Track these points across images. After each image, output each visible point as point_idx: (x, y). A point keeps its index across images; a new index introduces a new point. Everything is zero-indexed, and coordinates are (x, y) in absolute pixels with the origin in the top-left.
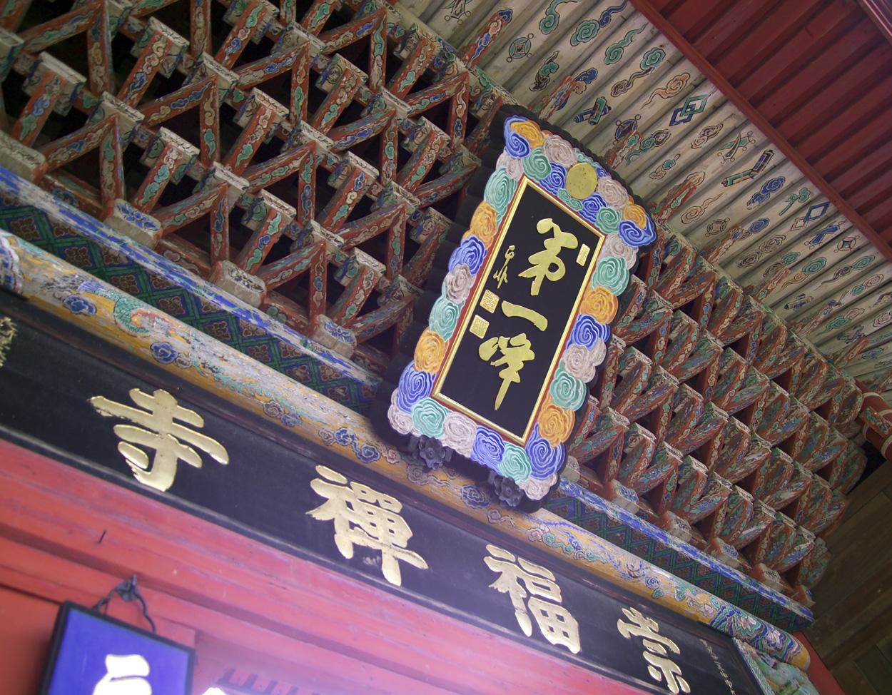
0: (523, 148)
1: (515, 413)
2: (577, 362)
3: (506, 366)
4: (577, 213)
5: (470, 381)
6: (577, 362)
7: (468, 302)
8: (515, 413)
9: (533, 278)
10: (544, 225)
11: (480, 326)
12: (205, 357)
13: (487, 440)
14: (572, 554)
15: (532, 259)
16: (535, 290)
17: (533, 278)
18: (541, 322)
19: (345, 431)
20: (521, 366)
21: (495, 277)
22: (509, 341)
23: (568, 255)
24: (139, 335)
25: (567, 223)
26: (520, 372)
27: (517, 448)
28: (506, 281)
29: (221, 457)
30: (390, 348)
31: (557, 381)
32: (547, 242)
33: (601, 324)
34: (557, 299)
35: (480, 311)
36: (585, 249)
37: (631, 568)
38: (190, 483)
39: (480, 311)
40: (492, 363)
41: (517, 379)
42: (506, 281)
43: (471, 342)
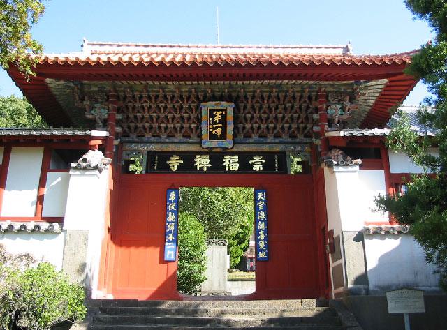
0: (204, 106)
1: (223, 137)
2: (230, 128)
5: (213, 137)
8: (223, 137)
10: (215, 113)
18: (221, 125)
30: (200, 136)
34: (223, 121)
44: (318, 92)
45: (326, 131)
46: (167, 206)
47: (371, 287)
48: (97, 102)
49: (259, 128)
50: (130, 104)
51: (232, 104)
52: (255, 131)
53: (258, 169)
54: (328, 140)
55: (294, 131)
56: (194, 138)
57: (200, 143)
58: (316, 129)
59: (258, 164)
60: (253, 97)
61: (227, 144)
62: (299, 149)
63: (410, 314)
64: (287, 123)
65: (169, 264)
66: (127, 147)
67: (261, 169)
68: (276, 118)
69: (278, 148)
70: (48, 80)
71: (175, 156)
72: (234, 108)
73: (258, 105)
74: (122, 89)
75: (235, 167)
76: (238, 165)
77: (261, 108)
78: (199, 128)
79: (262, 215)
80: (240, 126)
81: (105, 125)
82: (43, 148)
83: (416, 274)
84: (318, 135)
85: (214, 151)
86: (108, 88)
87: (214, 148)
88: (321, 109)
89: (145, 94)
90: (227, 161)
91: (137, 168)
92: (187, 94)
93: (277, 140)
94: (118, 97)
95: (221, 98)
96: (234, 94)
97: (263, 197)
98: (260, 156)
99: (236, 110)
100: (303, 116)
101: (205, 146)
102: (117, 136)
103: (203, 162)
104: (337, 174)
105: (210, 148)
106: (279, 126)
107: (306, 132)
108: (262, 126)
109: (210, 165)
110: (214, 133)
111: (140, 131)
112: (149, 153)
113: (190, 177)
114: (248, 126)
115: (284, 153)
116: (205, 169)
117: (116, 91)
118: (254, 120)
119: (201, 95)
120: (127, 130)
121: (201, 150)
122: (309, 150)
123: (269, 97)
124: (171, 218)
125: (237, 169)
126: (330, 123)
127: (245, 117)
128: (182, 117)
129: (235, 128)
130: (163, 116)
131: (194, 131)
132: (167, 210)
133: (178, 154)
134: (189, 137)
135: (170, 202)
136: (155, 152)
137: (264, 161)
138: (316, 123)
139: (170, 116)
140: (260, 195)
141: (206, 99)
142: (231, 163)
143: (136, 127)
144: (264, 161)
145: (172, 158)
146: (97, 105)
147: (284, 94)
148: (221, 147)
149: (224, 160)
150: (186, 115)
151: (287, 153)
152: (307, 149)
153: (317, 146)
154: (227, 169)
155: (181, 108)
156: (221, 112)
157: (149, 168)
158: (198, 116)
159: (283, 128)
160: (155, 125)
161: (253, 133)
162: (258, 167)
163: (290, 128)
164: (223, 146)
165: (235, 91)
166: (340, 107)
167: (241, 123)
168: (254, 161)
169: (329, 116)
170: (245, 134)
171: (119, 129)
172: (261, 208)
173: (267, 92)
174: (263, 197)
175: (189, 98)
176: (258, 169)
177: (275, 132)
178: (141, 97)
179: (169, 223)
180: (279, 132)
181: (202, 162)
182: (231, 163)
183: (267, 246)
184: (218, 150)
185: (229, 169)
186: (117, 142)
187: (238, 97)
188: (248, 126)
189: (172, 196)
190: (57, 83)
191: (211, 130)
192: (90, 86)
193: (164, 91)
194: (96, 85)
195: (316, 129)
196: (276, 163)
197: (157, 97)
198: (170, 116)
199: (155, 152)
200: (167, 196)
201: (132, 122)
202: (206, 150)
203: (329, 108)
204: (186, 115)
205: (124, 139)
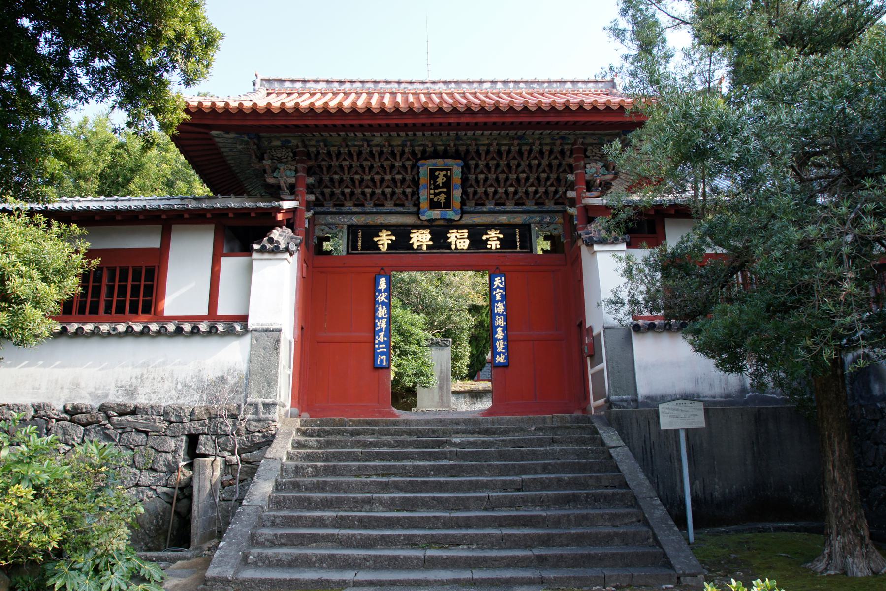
0: (423, 165)
1: (448, 205)
2: (457, 193)
5: (434, 205)
6: (457, 193)
10: (436, 174)
18: (445, 190)
25: (442, 170)
29: (394, 238)
30: (417, 204)
34: (448, 184)
43: (431, 200)
44: (573, 144)
45: (584, 198)
46: (375, 297)
47: (640, 398)
48: (280, 160)
49: (495, 192)
50: (324, 163)
51: (460, 162)
52: (491, 197)
53: (494, 247)
54: (587, 208)
55: (540, 197)
57: (417, 214)
58: (571, 194)
59: (493, 240)
60: (488, 152)
62: (548, 219)
63: (687, 431)
64: (532, 185)
65: (381, 371)
66: (322, 219)
67: (498, 246)
68: (518, 180)
69: (519, 219)
70: (214, 133)
71: (384, 231)
72: (462, 168)
73: (495, 162)
74: (313, 143)
75: (464, 244)
76: (467, 242)
77: (498, 166)
78: (416, 193)
79: (500, 308)
80: (470, 190)
81: (293, 190)
82: (213, 226)
83: (697, 382)
84: (573, 202)
85: (437, 223)
86: (294, 142)
87: (436, 219)
88: (577, 168)
89: (344, 150)
91: (336, 245)
92: (400, 148)
93: (520, 209)
94: (308, 154)
95: (445, 155)
96: (463, 149)
97: (501, 283)
98: (496, 229)
99: (466, 169)
100: (553, 176)
101: (423, 218)
102: (309, 206)
103: (421, 238)
104: (598, 255)
106: (521, 190)
107: (557, 196)
108: (500, 190)
109: (431, 243)
110: (435, 200)
111: (338, 198)
112: (349, 227)
113: (404, 257)
114: (481, 190)
115: (529, 225)
116: (424, 248)
117: (305, 146)
118: (489, 182)
120: (320, 197)
121: (419, 222)
122: (562, 220)
123: (509, 152)
124: (382, 312)
125: (466, 247)
126: (589, 186)
127: (476, 179)
128: (393, 180)
129: (465, 192)
130: (369, 178)
132: (375, 302)
133: (387, 227)
134: (403, 205)
135: (380, 291)
136: (357, 226)
137: (501, 236)
138: (572, 186)
139: (377, 178)
140: (497, 281)
141: (425, 156)
142: (459, 240)
143: (332, 194)
144: (501, 236)
145: (380, 234)
146: (282, 167)
149: (449, 235)
150: (399, 177)
151: (532, 226)
152: (559, 219)
153: (572, 216)
154: (453, 247)
156: (445, 173)
157: (352, 245)
158: (414, 178)
159: (526, 193)
162: (494, 244)
163: (536, 192)
165: (463, 145)
166: (602, 164)
167: (471, 186)
169: (587, 177)
171: (312, 198)
172: (498, 298)
174: (501, 283)
175: (403, 153)
176: (494, 247)
177: (517, 197)
178: (339, 154)
179: (379, 319)
180: (521, 197)
181: (420, 239)
182: (459, 240)
183: (506, 348)
184: (441, 222)
185: (456, 248)
186: (309, 214)
187: (467, 152)
188: (481, 190)
189: (383, 284)
190: (227, 136)
191: (432, 196)
192: (270, 140)
193: (368, 145)
194: (278, 139)
195: (571, 194)
196: (516, 238)
197: (360, 153)
198: (377, 178)
200: (376, 283)
201: (326, 187)
202: (426, 223)
203: (588, 166)
204: (399, 177)
205: (320, 209)
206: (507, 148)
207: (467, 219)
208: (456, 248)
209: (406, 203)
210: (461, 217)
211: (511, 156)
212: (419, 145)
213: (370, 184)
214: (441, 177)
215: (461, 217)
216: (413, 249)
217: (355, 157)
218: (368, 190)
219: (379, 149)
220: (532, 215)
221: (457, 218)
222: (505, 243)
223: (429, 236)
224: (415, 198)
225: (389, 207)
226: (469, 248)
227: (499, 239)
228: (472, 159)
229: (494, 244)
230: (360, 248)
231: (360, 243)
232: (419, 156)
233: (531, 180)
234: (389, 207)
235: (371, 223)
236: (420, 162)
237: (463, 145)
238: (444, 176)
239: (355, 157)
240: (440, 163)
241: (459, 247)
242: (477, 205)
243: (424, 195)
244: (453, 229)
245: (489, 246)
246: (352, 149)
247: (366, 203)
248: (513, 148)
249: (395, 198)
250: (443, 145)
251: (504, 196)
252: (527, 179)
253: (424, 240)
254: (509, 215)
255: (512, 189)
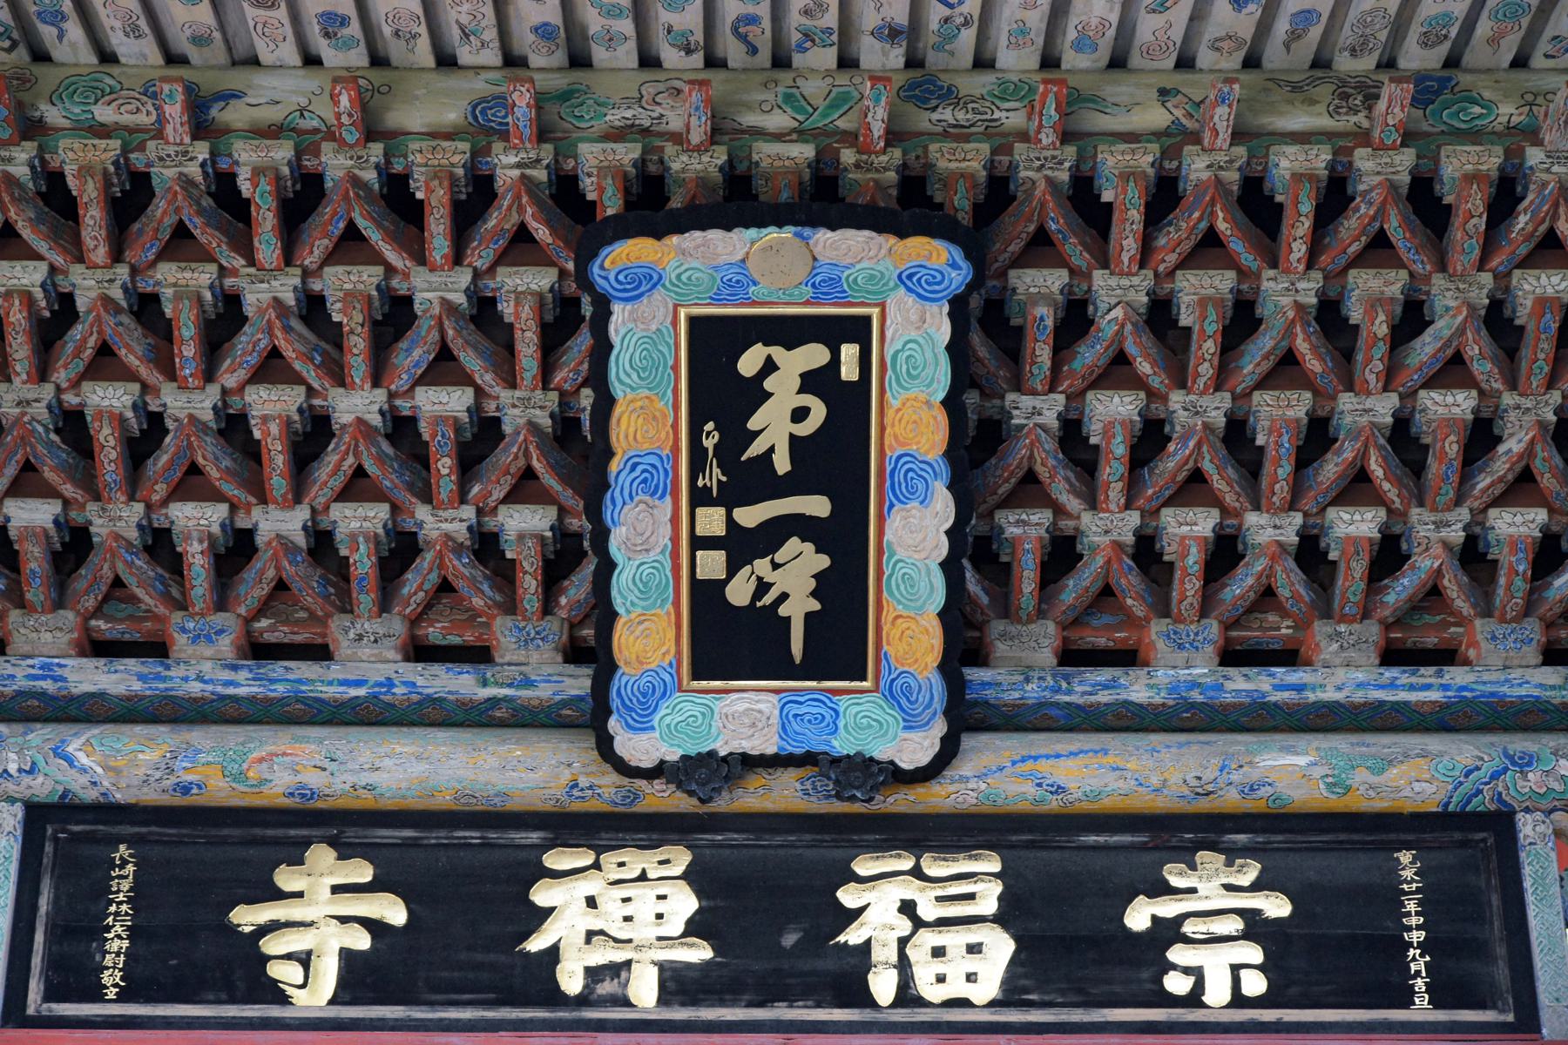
0: (643, 282)
2: (914, 536)
3: (784, 597)
4: (807, 303)
5: (729, 641)
6: (914, 536)
7: (675, 540)
9: (772, 449)
10: (749, 363)
11: (712, 564)
12: (351, 779)
13: (803, 710)
14: (1054, 804)
15: (753, 424)
16: (782, 464)
17: (772, 449)
18: (817, 506)
19: (576, 785)
20: (813, 583)
21: (700, 483)
22: (772, 561)
23: (817, 382)
24: (264, 789)
25: (789, 332)
26: (814, 594)
27: (865, 698)
28: (724, 479)
29: (394, 912)
30: (591, 649)
31: (891, 576)
32: (769, 384)
33: (929, 458)
34: (838, 453)
35: (698, 543)
36: (849, 352)
37: (1195, 783)
38: (358, 978)
39: (698, 543)
40: (759, 604)
41: (815, 606)
42: (724, 479)
43: (706, 596)
49: (1225, 553)
51: (939, 258)
52: (1188, 587)
53: (1217, 993)
56: (535, 668)
57: (592, 719)
59: (1214, 932)
60: (1164, 196)
61: (878, 723)
67: (1255, 984)
71: (321, 856)
72: (958, 308)
73: (1222, 282)
75: (974, 967)
76: (1001, 947)
77: (1242, 319)
78: (577, 552)
80: (1025, 529)
87: (750, 763)
90: (878, 904)
92: (456, 155)
93: (1421, 688)
95: (822, 200)
98: (1232, 855)
99: (985, 331)
105: (705, 770)
106: (1434, 534)
109: (699, 953)
110: (739, 592)
114: (1107, 528)
115: (1501, 823)
116: (644, 990)
118: (1172, 463)
119: (600, 165)
121: (606, 790)
123: (1335, 195)
125: (987, 989)
127: (1072, 436)
129: (973, 552)
131: (530, 585)
133: (344, 826)
136: (108, 812)
137: (1276, 907)
139: (271, 407)
141: (652, 206)
144: (1276, 907)
145: (286, 879)
147: (1491, 160)
148: (808, 759)
149: (848, 897)
150: (441, 405)
154: (883, 986)
155: (394, 316)
158: (566, 428)
160: (117, 520)
161: (1163, 609)
164: (842, 745)
165: (957, 134)
168: (1168, 908)
170: (1076, 621)
173: (1302, 138)
175: (475, 196)
176: (1217, 993)
180: (1433, 593)
181: (610, 917)
184: (784, 793)
185: (907, 996)
187: (999, 192)
188: (1107, 528)
191: (712, 564)
193: (201, 128)
197: (131, 197)
198: (271, 407)
199: (111, 814)
202: (661, 797)
204: (441, 405)
206: (1319, 159)
207: (996, 774)
208: (907, 996)
209: (504, 634)
210: (948, 753)
211: (1351, 229)
212: (617, 135)
213: (214, 461)
214: (784, 390)
215: (948, 753)
216: (554, 997)
217: (93, 221)
218: (196, 520)
219: (282, 153)
220: (1520, 744)
221: (916, 750)
222: (1320, 956)
223: (685, 903)
224: (577, 589)
225: (367, 658)
226: (1011, 995)
227: (1255, 927)
228: (1041, 248)
229: (1216, 965)
230: (111, 979)
231: (117, 942)
232: (612, 205)
233: (1513, 444)
234: (367, 658)
235: (219, 790)
236: (623, 256)
237: (957, 134)
238: (811, 382)
239: (93, 221)
240: (765, 265)
241: (933, 993)
242: (1072, 657)
243: (647, 546)
244: (882, 847)
245: (1177, 984)
246: (71, 156)
247: (181, 632)
248: (1364, 160)
249: (416, 583)
250: (801, 134)
251: (1291, 583)
252: (1481, 436)
253: (645, 931)
254: (1341, 743)
255: (1356, 525)
